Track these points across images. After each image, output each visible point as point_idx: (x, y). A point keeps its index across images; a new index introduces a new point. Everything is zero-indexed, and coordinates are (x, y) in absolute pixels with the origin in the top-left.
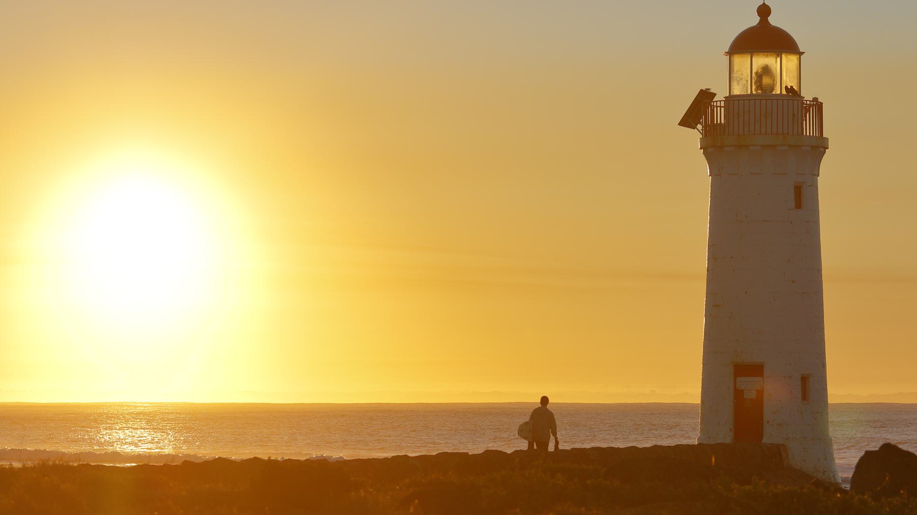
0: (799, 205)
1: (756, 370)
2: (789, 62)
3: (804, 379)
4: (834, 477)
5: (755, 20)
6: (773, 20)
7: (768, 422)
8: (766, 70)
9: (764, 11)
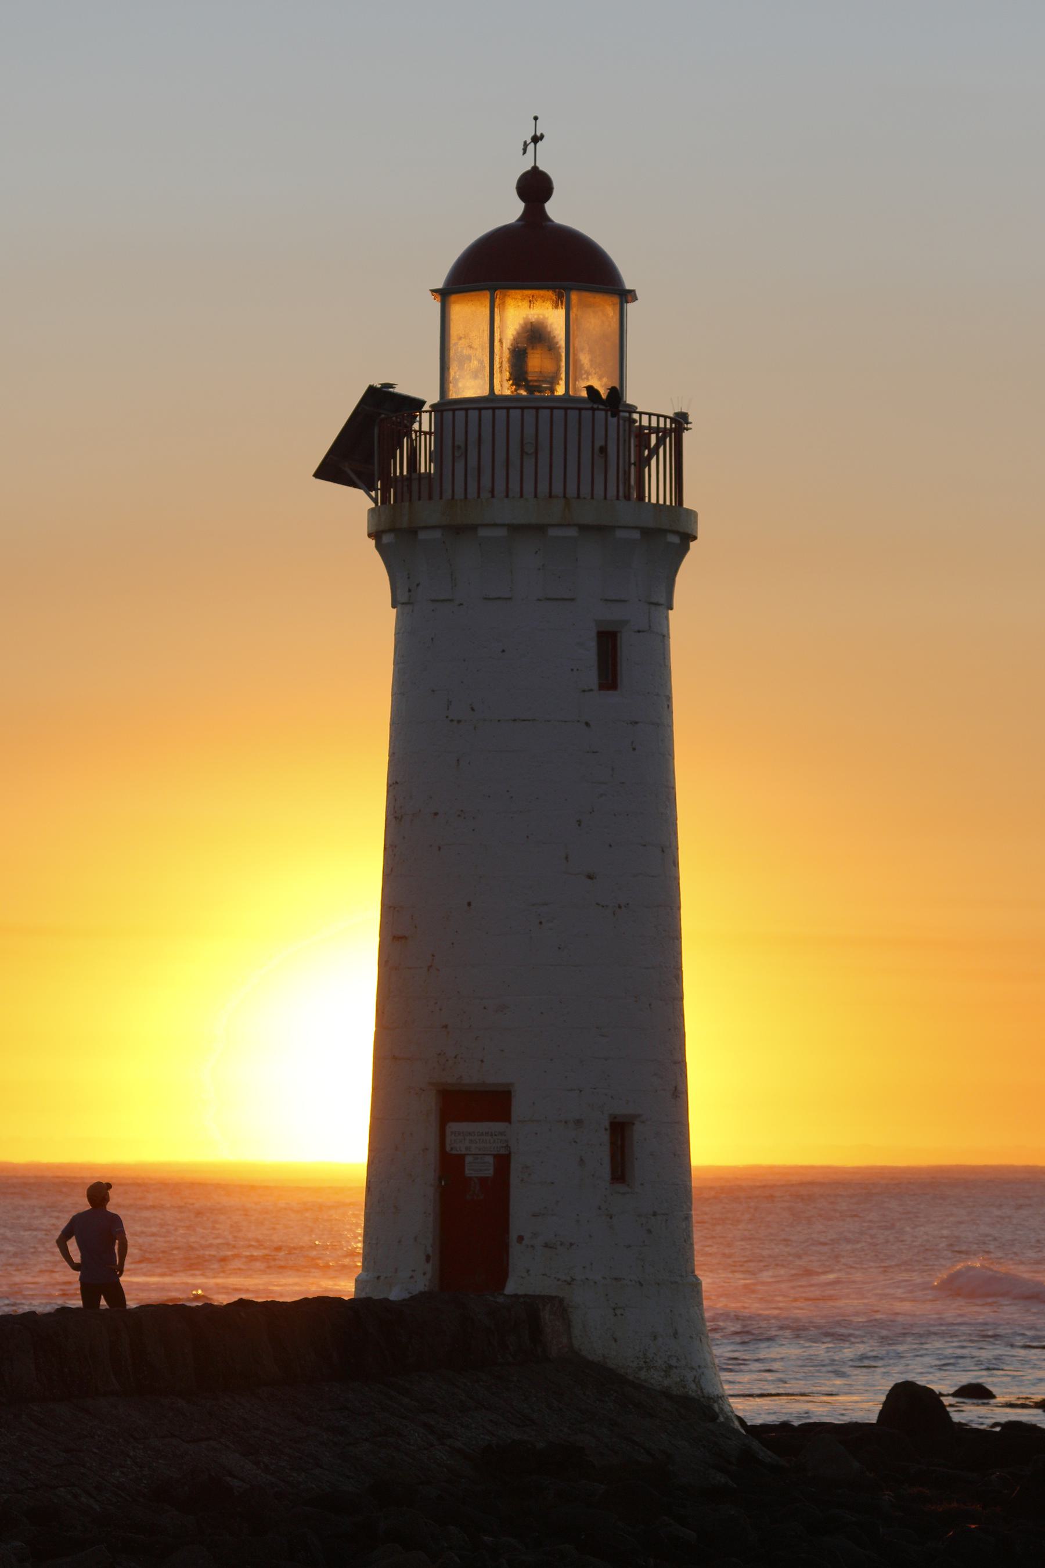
0: (609, 676)
1: (492, 1104)
2: (596, 317)
3: (620, 1130)
4: (696, 1380)
5: (511, 210)
6: (557, 211)
7: (521, 1239)
8: (535, 336)
9: (535, 187)
